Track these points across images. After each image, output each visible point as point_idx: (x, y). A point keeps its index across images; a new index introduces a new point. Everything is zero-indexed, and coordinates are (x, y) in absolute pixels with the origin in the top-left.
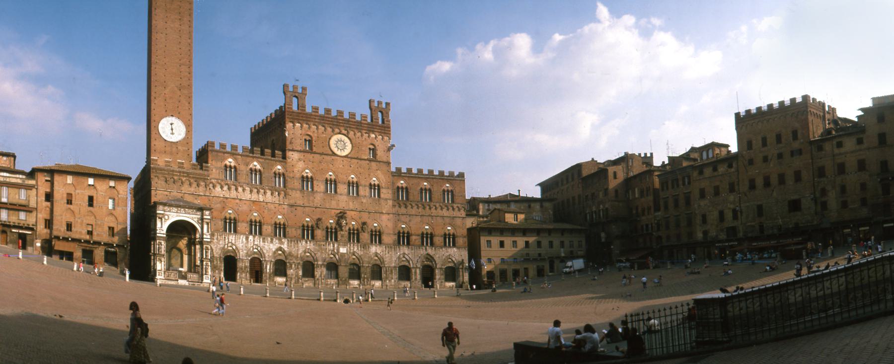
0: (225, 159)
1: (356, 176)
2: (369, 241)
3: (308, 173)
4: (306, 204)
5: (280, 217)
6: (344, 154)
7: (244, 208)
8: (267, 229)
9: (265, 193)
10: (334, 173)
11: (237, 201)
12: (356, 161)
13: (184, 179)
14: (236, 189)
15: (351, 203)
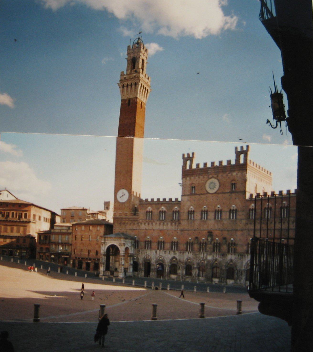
0: (147, 208)
1: (221, 206)
2: (226, 251)
3: (192, 208)
4: (190, 228)
5: (175, 238)
6: (214, 191)
7: (156, 234)
8: (168, 246)
9: (167, 224)
10: (207, 206)
11: (152, 231)
12: (221, 195)
13: (127, 222)
14: (152, 224)
15: (216, 225)
